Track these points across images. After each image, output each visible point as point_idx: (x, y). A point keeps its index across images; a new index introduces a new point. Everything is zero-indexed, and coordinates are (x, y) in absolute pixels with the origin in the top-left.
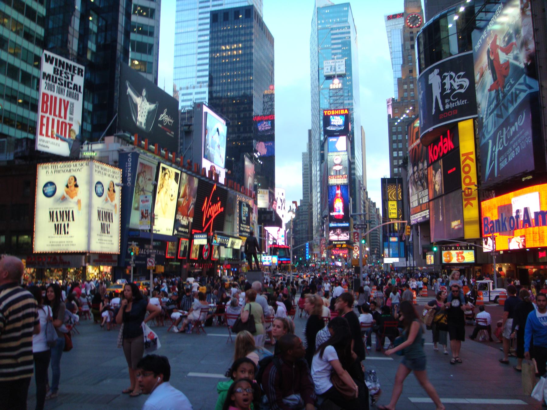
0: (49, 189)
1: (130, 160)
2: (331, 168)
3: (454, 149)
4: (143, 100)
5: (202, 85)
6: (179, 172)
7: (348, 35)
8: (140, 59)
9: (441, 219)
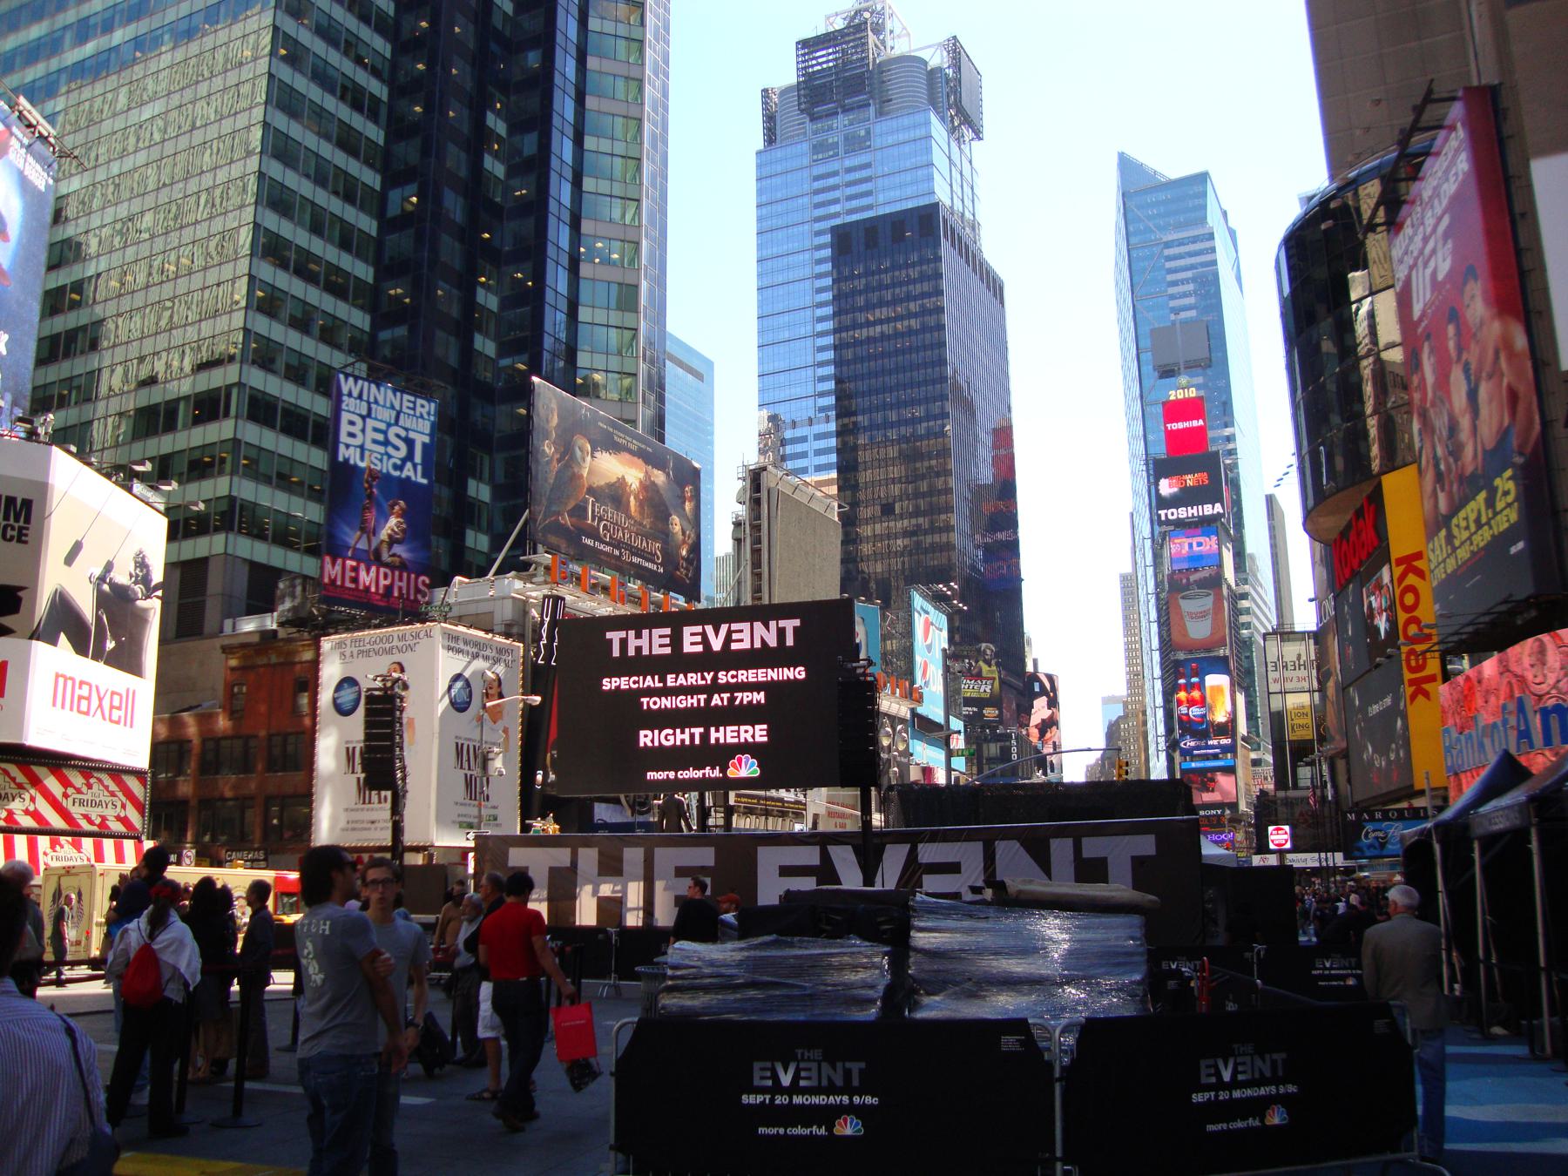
7: (1208, 258)
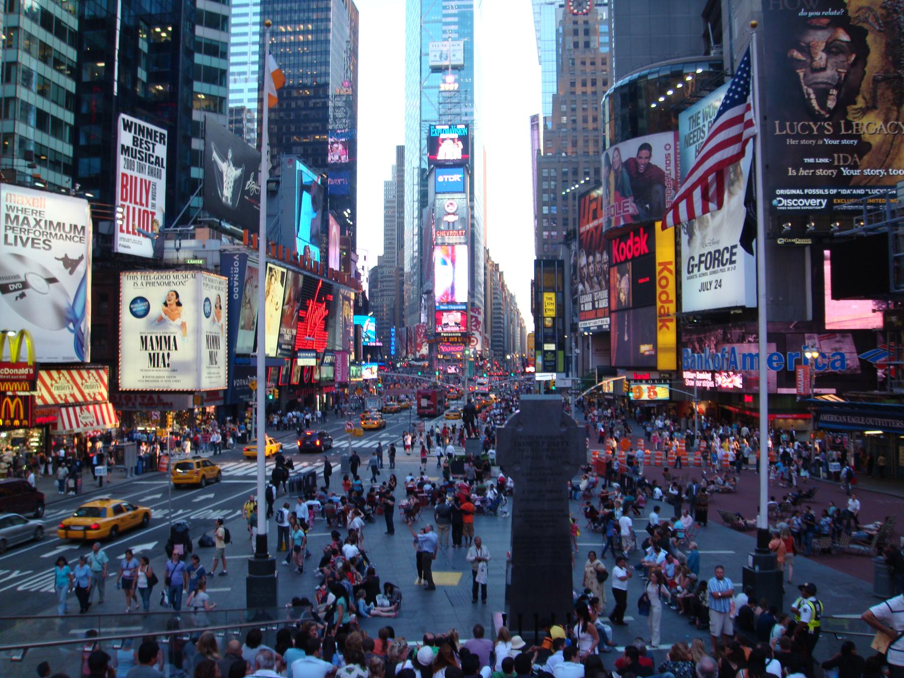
0: (139, 307)
1: (236, 264)
2: (440, 220)
3: (648, 254)
5: (237, 77)
6: (285, 270)
8: (207, 92)
9: (626, 338)
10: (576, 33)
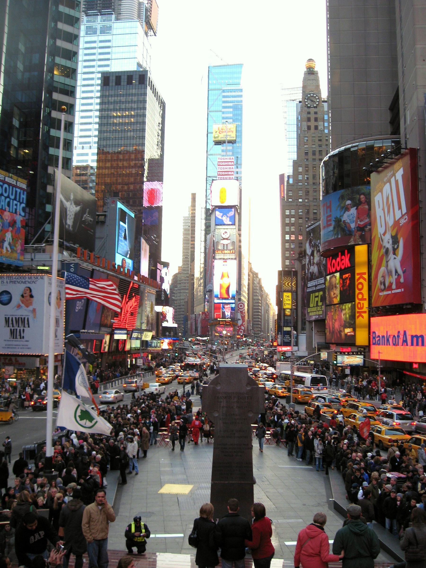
3: (350, 267)
4: (71, 204)
7: (239, 99)
10: (309, 120)
